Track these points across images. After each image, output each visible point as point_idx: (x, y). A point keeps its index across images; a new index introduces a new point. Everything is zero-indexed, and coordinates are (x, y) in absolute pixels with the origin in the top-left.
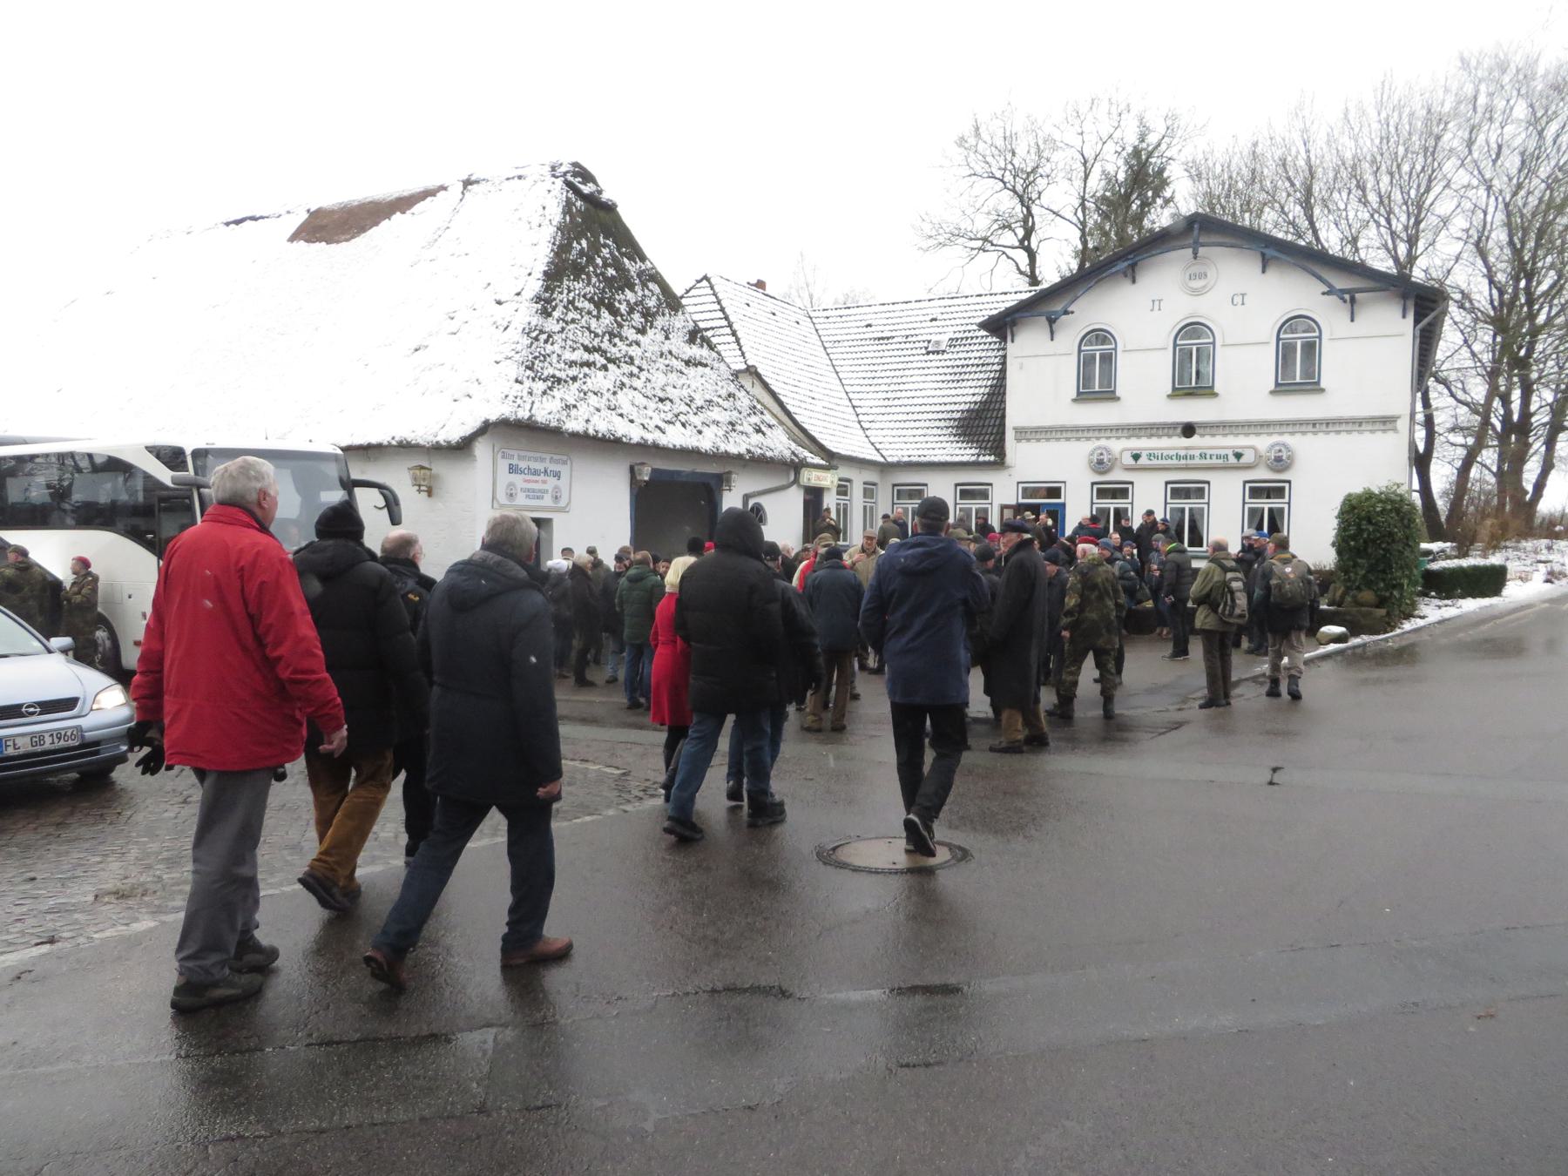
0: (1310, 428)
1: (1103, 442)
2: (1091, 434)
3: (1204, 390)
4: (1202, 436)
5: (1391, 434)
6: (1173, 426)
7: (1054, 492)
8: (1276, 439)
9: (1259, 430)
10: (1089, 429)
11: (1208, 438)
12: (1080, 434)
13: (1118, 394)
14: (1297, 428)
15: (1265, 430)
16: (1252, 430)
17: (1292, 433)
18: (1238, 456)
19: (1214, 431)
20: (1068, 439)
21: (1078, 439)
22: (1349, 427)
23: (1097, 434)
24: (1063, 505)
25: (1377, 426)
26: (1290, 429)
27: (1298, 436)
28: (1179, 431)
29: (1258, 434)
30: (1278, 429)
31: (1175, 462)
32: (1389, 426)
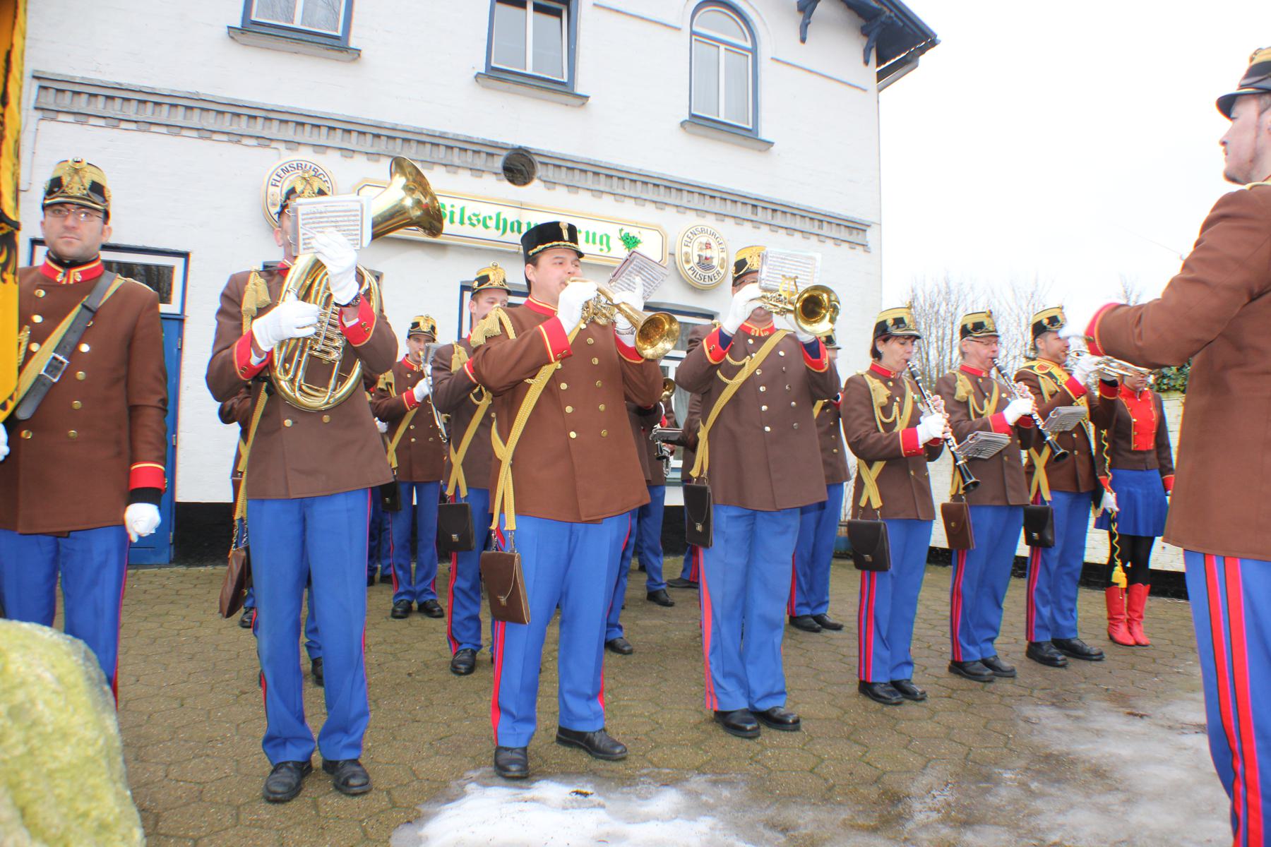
0: (747, 213)
1: (305, 155)
2: (274, 130)
3: (562, 89)
4: (550, 184)
5: (860, 248)
6: (485, 149)
7: (158, 279)
8: (691, 220)
9: (662, 195)
10: (269, 115)
11: (561, 191)
12: (242, 126)
13: (353, 43)
14: (729, 208)
15: (673, 198)
16: (650, 193)
17: (721, 216)
18: (630, 241)
19: (577, 178)
20: (205, 133)
21: (237, 138)
22: (806, 225)
23: (289, 132)
24: (179, 320)
25: (844, 234)
26: (717, 206)
27: (729, 222)
28: (498, 163)
29: (660, 205)
30: (696, 201)
31: (493, 234)
32: (854, 237)
